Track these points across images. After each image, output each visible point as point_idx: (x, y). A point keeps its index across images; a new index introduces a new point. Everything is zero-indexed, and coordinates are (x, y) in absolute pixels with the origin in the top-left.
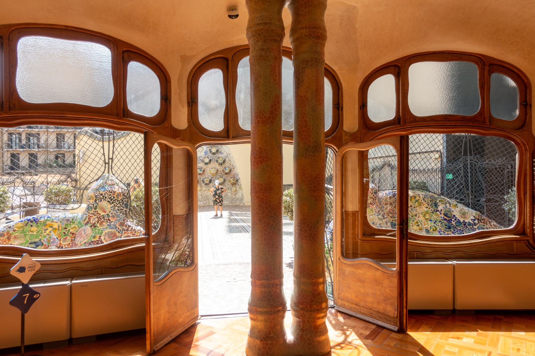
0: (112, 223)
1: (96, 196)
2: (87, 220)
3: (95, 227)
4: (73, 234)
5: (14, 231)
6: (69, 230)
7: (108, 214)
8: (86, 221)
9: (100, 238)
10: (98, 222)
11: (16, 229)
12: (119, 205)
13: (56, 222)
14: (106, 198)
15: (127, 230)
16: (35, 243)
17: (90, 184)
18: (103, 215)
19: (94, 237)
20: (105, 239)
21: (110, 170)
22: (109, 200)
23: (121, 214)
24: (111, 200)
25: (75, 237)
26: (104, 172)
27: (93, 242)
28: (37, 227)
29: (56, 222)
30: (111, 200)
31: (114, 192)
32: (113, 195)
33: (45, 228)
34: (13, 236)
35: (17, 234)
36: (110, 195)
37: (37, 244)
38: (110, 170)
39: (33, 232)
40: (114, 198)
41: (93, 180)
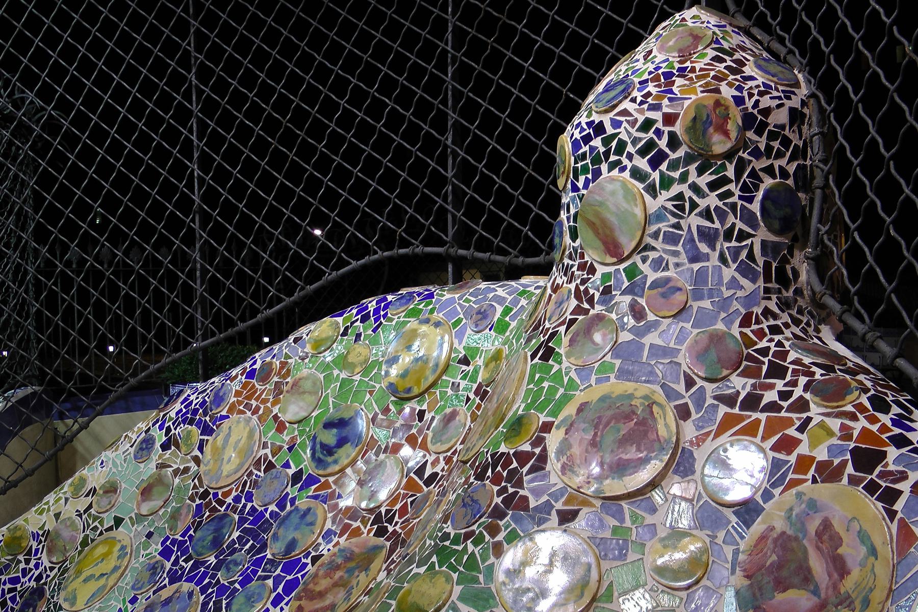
12: (712, 200)
14: (622, 145)
22: (642, 163)
23: (729, 272)
30: (655, 163)
36: (647, 125)
40: (674, 142)
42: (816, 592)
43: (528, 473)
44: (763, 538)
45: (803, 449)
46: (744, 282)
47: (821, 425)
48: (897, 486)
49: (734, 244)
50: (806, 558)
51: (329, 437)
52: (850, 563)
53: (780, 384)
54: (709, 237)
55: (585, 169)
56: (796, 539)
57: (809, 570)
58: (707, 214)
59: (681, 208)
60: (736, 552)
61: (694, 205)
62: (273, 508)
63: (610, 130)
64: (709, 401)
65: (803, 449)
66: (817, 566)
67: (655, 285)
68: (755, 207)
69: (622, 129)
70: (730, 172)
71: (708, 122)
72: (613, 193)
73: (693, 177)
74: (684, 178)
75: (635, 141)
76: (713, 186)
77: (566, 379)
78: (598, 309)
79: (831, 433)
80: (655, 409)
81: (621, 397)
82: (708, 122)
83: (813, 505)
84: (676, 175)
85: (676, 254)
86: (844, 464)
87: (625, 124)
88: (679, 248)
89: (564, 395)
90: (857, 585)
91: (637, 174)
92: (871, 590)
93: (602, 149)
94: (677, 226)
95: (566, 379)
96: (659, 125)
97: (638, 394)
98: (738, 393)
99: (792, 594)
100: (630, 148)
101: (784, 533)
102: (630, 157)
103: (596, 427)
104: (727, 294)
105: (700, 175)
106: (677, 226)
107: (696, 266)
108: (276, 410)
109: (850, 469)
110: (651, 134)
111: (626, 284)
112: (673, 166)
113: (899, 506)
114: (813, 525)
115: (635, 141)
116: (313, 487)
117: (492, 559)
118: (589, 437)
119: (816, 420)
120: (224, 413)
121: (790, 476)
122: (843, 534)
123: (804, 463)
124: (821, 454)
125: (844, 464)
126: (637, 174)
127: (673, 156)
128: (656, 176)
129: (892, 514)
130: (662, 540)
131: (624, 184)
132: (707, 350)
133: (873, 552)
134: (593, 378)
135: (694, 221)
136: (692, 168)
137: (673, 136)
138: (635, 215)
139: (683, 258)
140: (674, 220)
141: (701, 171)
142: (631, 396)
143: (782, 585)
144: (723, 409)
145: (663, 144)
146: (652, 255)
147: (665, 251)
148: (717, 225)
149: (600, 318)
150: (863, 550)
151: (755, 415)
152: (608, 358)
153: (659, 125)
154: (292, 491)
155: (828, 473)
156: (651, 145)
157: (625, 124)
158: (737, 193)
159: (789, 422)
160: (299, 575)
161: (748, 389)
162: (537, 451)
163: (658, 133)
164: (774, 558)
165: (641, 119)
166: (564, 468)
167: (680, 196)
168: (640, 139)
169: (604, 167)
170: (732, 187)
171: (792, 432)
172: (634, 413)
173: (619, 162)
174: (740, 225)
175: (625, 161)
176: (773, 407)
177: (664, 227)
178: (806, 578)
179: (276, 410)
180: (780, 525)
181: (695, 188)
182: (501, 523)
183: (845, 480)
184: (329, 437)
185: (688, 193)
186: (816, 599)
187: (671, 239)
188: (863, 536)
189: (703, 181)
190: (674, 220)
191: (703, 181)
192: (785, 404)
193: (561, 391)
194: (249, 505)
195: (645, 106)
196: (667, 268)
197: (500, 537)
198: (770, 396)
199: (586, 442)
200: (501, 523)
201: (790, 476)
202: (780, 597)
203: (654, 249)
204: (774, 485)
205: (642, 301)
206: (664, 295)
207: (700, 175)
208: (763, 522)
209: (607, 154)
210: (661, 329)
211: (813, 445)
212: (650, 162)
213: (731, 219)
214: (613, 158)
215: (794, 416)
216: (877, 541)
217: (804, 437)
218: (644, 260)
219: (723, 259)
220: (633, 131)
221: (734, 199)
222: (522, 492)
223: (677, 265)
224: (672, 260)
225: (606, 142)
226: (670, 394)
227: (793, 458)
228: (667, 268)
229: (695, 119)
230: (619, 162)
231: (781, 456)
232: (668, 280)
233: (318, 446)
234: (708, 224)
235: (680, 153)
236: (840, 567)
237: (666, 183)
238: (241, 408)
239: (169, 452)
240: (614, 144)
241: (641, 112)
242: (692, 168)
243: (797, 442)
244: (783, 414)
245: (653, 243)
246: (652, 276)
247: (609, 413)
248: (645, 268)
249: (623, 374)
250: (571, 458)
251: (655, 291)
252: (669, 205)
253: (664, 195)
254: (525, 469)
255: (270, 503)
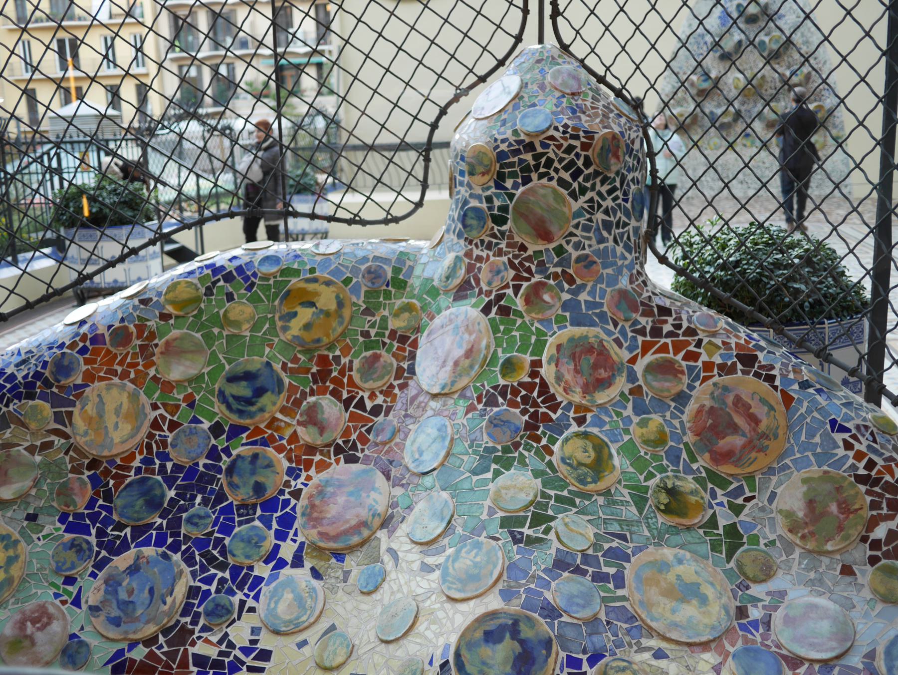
0: (583, 297)
1: (501, 156)
2: (462, 272)
3: (505, 311)
4: (403, 339)
5: (165, 317)
6: (384, 319)
7: (560, 251)
8: (457, 281)
9: (534, 374)
10: (517, 289)
11: (170, 309)
12: (609, 203)
13: (328, 283)
14: (549, 162)
15: (656, 332)
16: (248, 376)
17: (456, 99)
18: (538, 253)
19: (509, 367)
20: (559, 378)
21: (548, 23)
22: (566, 176)
23: (620, 249)
24: (575, 176)
25: (413, 356)
26: (518, 39)
27: (503, 392)
28: (255, 300)
29: (328, 283)
30: (575, 176)
31: (590, 135)
32: (585, 147)
33: (285, 310)
34: (161, 342)
35: (175, 333)
36: (570, 149)
37: (258, 383)
38: (548, 23)
39: (237, 324)
40: (588, 163)
41: (472, 79)
42: (744, 435)
43: (539, 397)
44: (699, 412)
45: (704, 357)
46: (627, 254)
47: (710, 343)
48: (772, 373)
49: (621, 230)
50: (732, 419)
51: (243, 389)
52: (759, 416)
53: (670, 320)
54: (607, 226)
55: (513, 175)
56: (721, 409)
57: (736, 424)
58: (606, 212)
59: (592, 207)
60: (682, 423)
61: (600, 206)
62: (203, 461)
63: (539, 150)
64: (630, 334)
65: (704, 357)
66: (739, 420)
67: (579, 260)
68: (629, 205)
69: (550, 150)
70: (618, 184)
71: (609, 150)
72: (544, 196)
73: (598, 187)
74: (593, 188)
75: (561, 160)
76: (610, 192)
77: (533, 329)
78: (537, 278)
79: (719, 348)
80: (605, 344)
81: (580, 338)
82: (609, 150)
83: (726, 389)
84: (588, 185)
85: (589, 238)
86: (734, 364)
87: (552, 147)
88: (591, 235)
89: (537, 340)
90: (768, 426)
91: (562, 183)
92: (777, 428)
93: (532, 163)
94: (590, 220)
95: (533, 329)
96: (578, 150)
97: (590, 335)
98: (644, 327)
99: (729, 439)
100: (556, 164)
101: (712, 407)
102: (556, 170)
103: (574, 360)
104: (620, 263)
105: (602, 184)
106: (590, 220)
107: (602, 246)
108: (152, 372)
109: (739, 366)
110: (572, 156)
111: (556, 260)
112: (586, 179)
113: (777, 382)
114: (730, 399)
115: (561, 160)
116: (244, 435)
117: (548, 458)
118: (572, 367)
119: (706, 340)
120: (79, 381)
121: (702, 375)
122: (750, 401)
123: (708, 366)
124: (718, 360)
125: (734, 364)
126: (562, 183)
127: (586, 172)
128: (575, 185)
129: (776, 388)
130: (638, 424)
131: (554, 191)
132: (619, 302)
133: (772, 408)
134: (555, 326)
135: (600, 216)
136: (598, 180)
137: (587, 158)
138: (564, 213)
139: (594, 242)
140: (588, 216)
141: (603, 183)
142: (586, 337)
143: (721, 435)
144: (640, 339)
145: (580, 163)
146: (574, 239)
147: (583, 237)
148: (612, 219)
149: (540, 284)
150: (766, 408)
151: (663, 340)
152: (560, 312)
153: (578, 150)
154: (221, 443)
155: (726, 369)
156: (572, 163)
157: (552, 147)
158: (621, 197)
159: (689, 343)
160: (287, 510)
161: (650, 324)
162: (537, 380)
163: (578, 155)
164: (710, 421)
165: (565, 144)
166: (565, 390)
167: (591, 200)
168: (564, 159)
169: (534, 176)
170: (618, 193)
171: (691, 348)
172: (592, 347)
173: (547, 174)
174: (624, 218)
175: (553, 174)
176: (670, 334)
177: (582, 221)
178: (735, 429)
179: (152, 372)
180: (708, 403)
181: (599, 194)
182: (539, 433)
183: (739, 373)
184: (243, 389)
185: (596, 198)
186: (744, 439)
187: (586, 229)
188: (763, 401)
189: (604, 189)
190: (588, 216)
191: (604, 189)
192: (680, 332)
193: (533, 339)
194: (169, 465)
195: (568, 135)
196: (584, 248)
197: (544, 442)
198: (667, 328)
199: (572, 372)
200: (539, 433)
201: (702, 375)
202: (722, 443)
203: (575, 235)
204: (694, 381)
205: (571, 271)
206: (585, 267)
207: (602, 184)
208: (696, 402)
209: (537, 167)
210: (588, 288)
211: (710, 355)
212: (571, 175)
213: (619, 214)
214: (542, 170)
215: (690, 339)
216: (773, 403)
217: (701, 350)
218: (568, 242)
219: (615, 241)
220: (559, 153)
221: (620, 201)
222: (541, 410)
223: (590, 246)
224: (587, 242)
225: (537, 157)
226: (609, 333)
227: (700, 363)
228: (584, 248)
229: (602, 148)
230: (547, 174)
231: (692, 363)
232: (587, 256)
233: (231, 400)
234: (607, 218)
235: (591, 170)
236: (754, 420)
237: (583, 190)
238: (102, 374)
239: (9, 431)
240: (543, 160)
241: (565, 139)
242: (598, 180)
243: (698, 355)
244: (681, 338)
245: (575, 231)
246: (575, 254)
247: (578, 350)
248: (570, 248)
249: (576, 323)
250: (566, 382)
251: (579, 265)
252: (585, 206)
253: (582, 199)
254: (535, 394)
255: (198, 457)
